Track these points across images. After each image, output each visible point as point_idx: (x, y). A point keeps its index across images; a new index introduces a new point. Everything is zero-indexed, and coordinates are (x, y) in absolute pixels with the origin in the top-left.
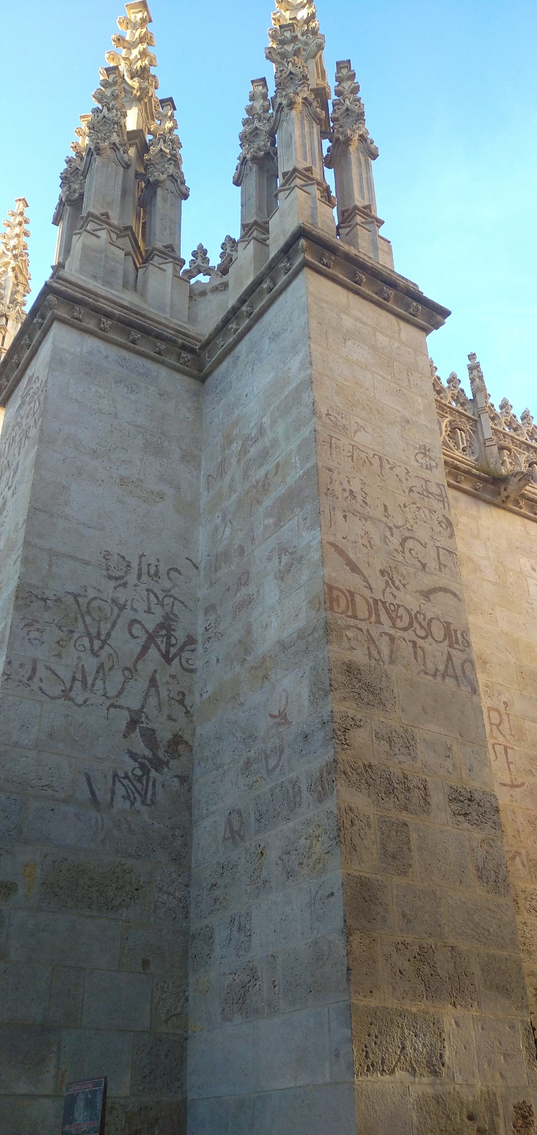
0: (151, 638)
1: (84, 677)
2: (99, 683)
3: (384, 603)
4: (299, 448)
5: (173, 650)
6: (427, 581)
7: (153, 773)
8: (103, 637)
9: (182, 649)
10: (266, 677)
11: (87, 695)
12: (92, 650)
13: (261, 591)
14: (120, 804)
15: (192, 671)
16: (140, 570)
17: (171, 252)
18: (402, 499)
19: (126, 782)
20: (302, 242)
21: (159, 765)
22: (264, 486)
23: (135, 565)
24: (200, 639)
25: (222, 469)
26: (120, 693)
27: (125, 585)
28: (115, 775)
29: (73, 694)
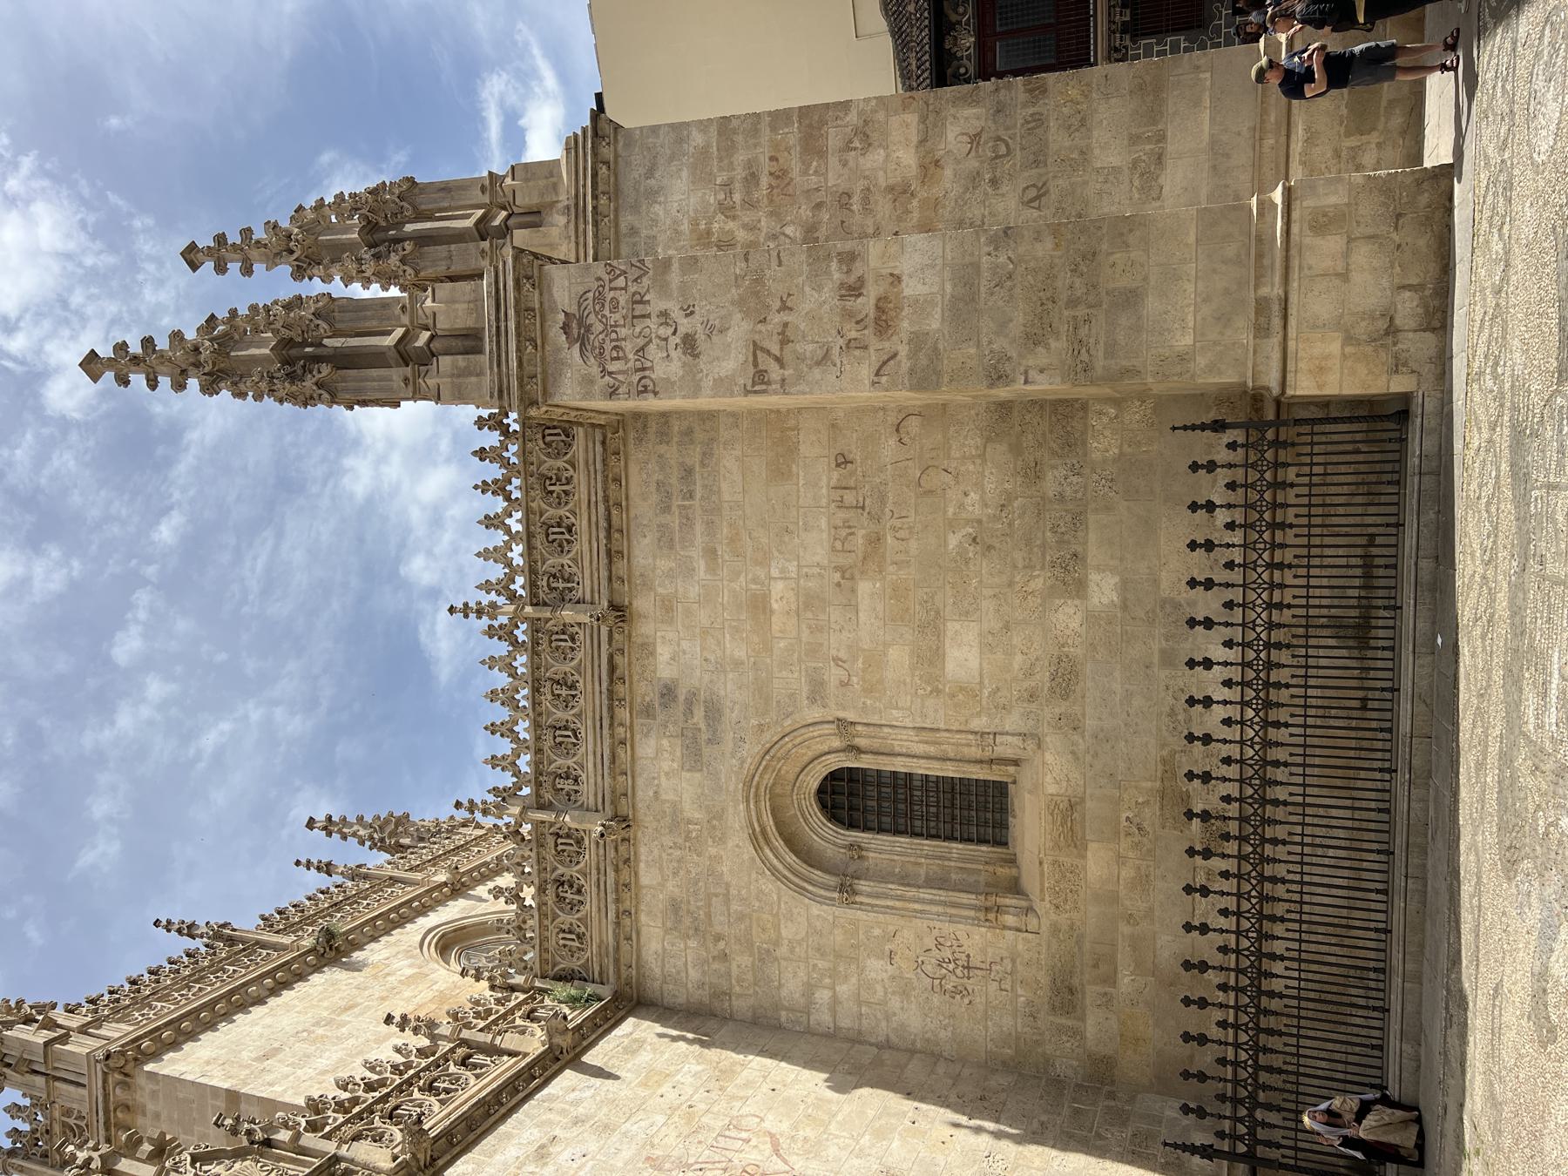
10: (937, 163)
22: (780, 175)
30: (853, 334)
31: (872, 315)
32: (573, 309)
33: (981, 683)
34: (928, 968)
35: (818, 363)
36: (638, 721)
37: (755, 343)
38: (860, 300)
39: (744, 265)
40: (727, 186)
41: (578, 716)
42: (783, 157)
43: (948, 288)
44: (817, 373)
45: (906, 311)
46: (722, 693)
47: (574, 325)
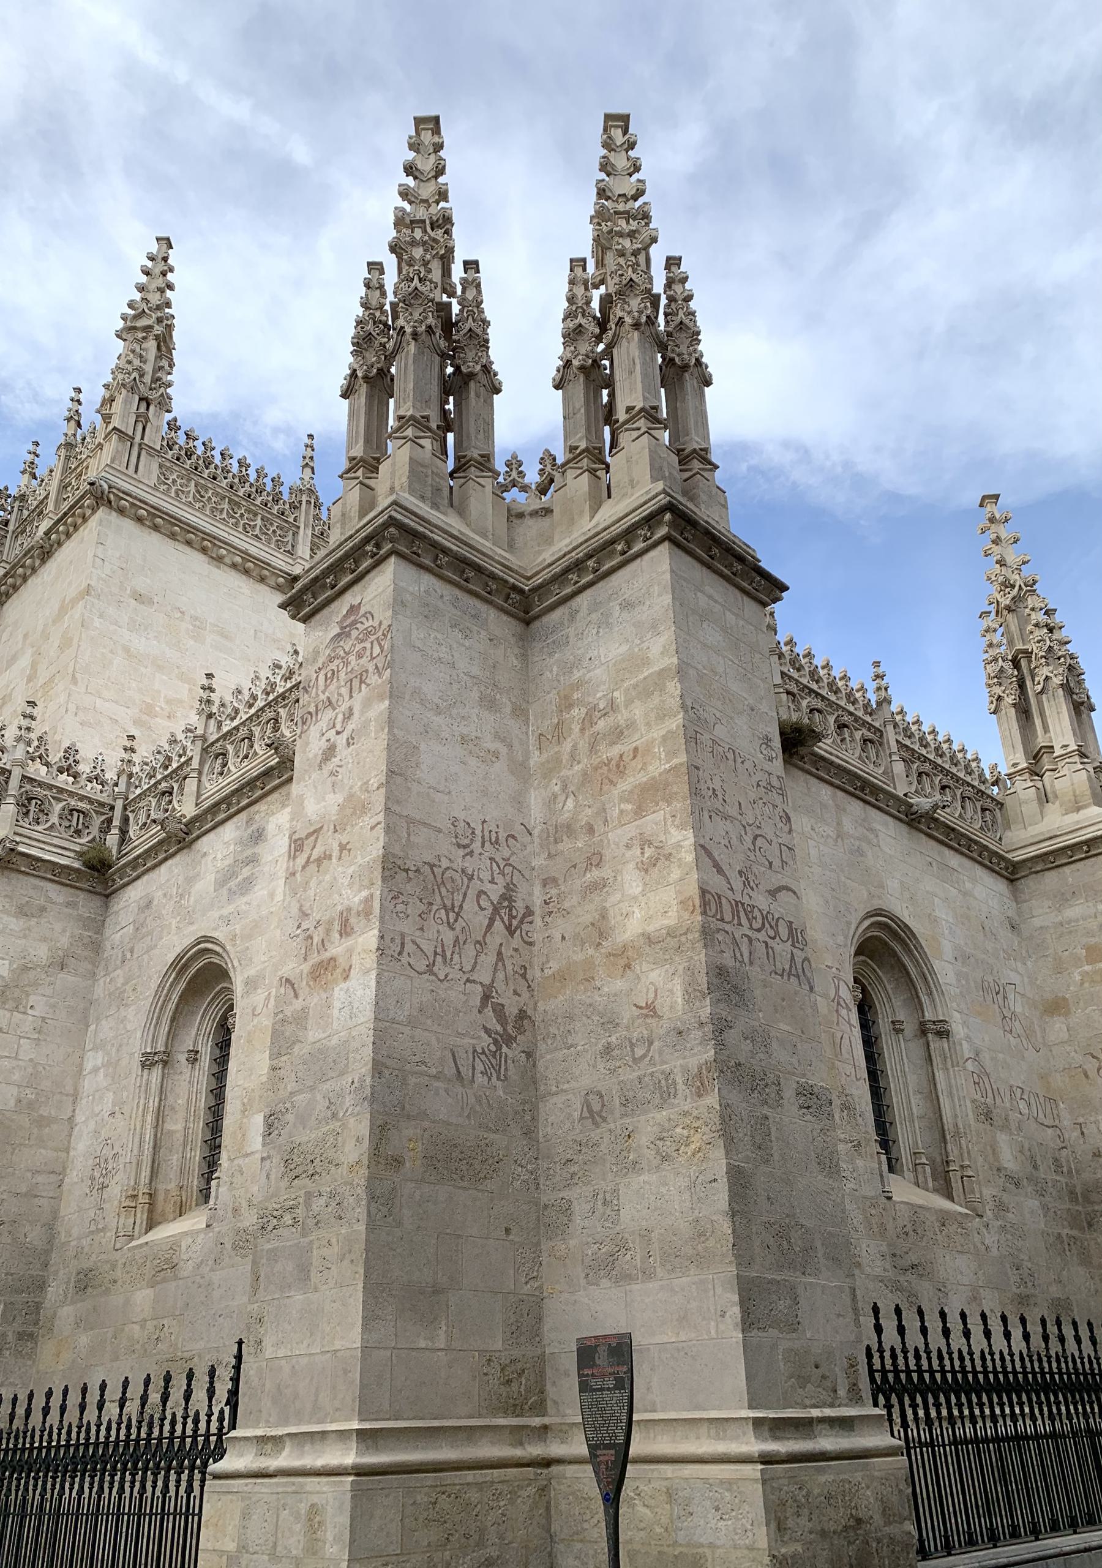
0: (496, 910)
1: (443, 951)
2: (456, 957)
3: (743, 904)
4: (664, 738)
5: (515, 923)
6: (776, 880)
7: (504, 1049)
8: (456, 910)
9: (521, 922)
10: (628, 966)
11: (447, 970)
12: (448, 923)
13: (619, 878)
14: (480, 1079)
15: (531, 944)
16: (483, 837)
17: (485, 462)
18: (752, 795)
19: (483, 1057)
20: (668, 516)
21: (509, 1040)
22: (620, 767)
23: (478, 832)
24: (538, 911)
25: (560, 731)
26: (474, 967)
27: (471, 853)
28: (475, 1051)
29: (435, 969)
30: (316, 940)
31: (327, 955)
32: (362, 611)
33: (247, 1155)
34: (104, 1152)
35: (300, 909)
36: (243, 816)
37: (322, 827)
38: (337, 936)
39: (376, 785)
40: (612, 706)
41: (256, 753)
42: (637, 764)
43: (334, 1041)
44: (295, 910)
45: (324, 996)
46: (256, 888)
47: (352, 618)
